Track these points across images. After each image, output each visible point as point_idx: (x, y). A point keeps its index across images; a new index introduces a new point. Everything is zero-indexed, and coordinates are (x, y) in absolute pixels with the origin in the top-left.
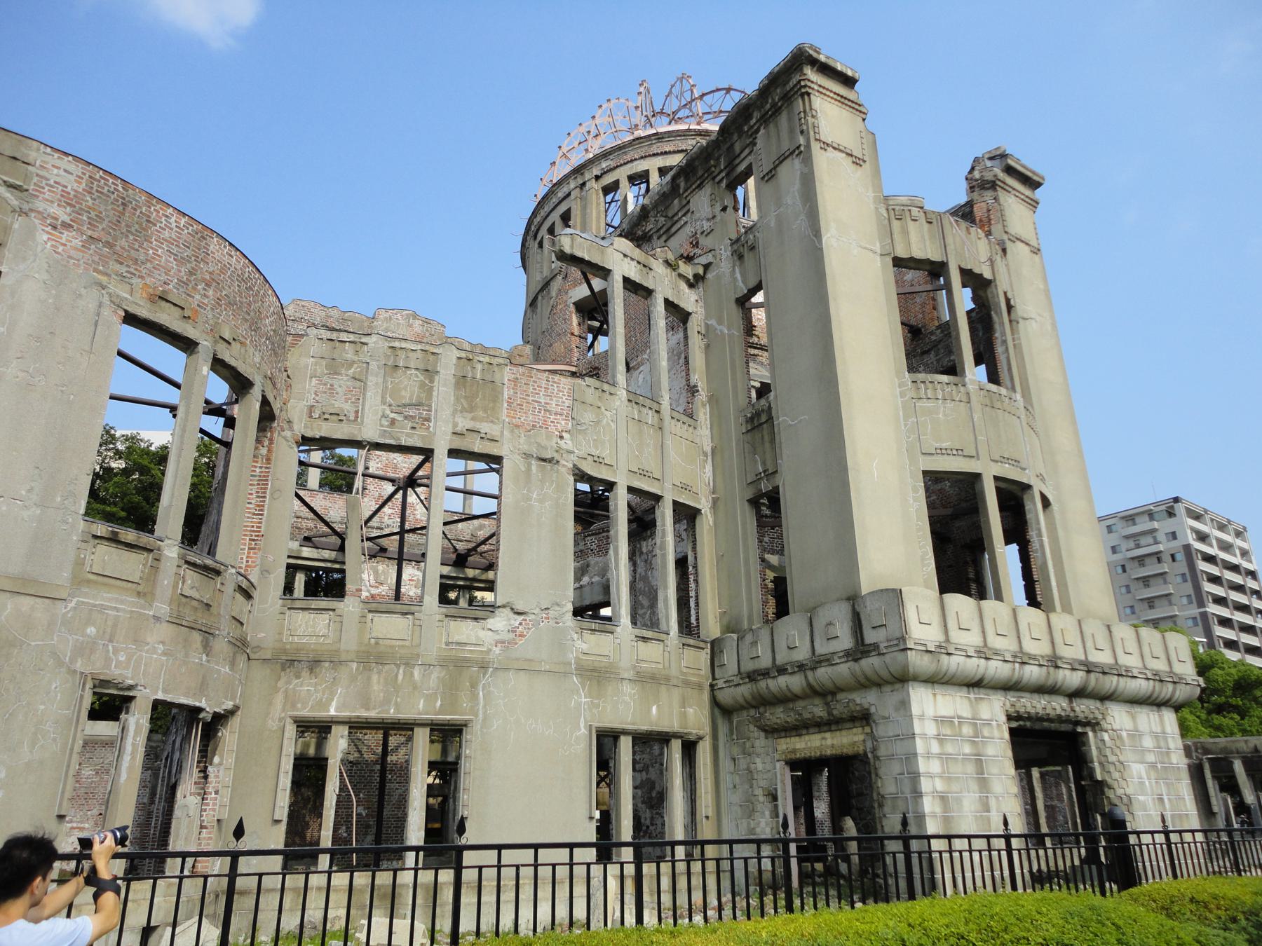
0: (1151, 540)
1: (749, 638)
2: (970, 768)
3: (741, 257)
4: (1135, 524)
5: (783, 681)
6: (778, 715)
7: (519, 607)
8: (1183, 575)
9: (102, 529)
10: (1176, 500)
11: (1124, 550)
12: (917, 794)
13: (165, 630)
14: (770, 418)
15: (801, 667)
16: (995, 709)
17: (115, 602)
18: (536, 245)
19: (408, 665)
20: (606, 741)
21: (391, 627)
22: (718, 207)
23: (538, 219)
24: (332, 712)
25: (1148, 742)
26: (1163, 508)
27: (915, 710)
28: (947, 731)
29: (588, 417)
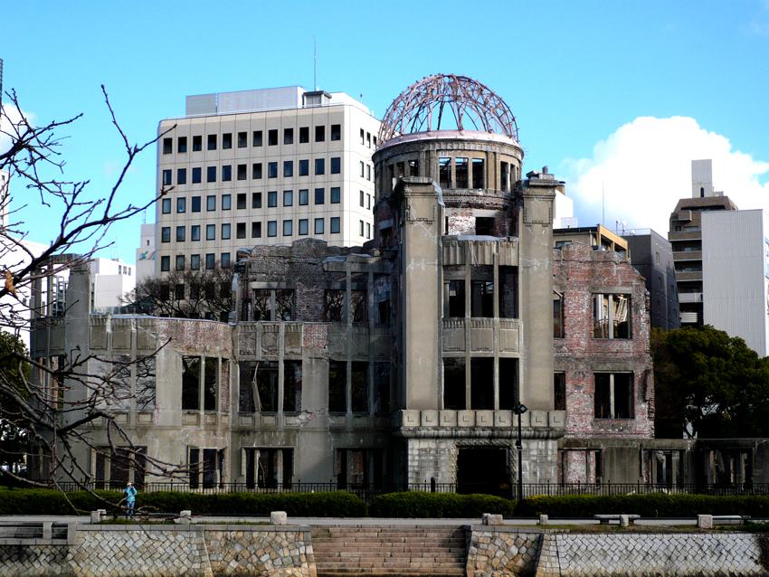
2: (431, 464)
7: (309, 411)
9: (186, 411)
13: (204, 433)
17: (191, 428)
19: (275, 432)
21: (269, 420)
25: (534, 453)
27: (410, 447)
29: (335, 339)
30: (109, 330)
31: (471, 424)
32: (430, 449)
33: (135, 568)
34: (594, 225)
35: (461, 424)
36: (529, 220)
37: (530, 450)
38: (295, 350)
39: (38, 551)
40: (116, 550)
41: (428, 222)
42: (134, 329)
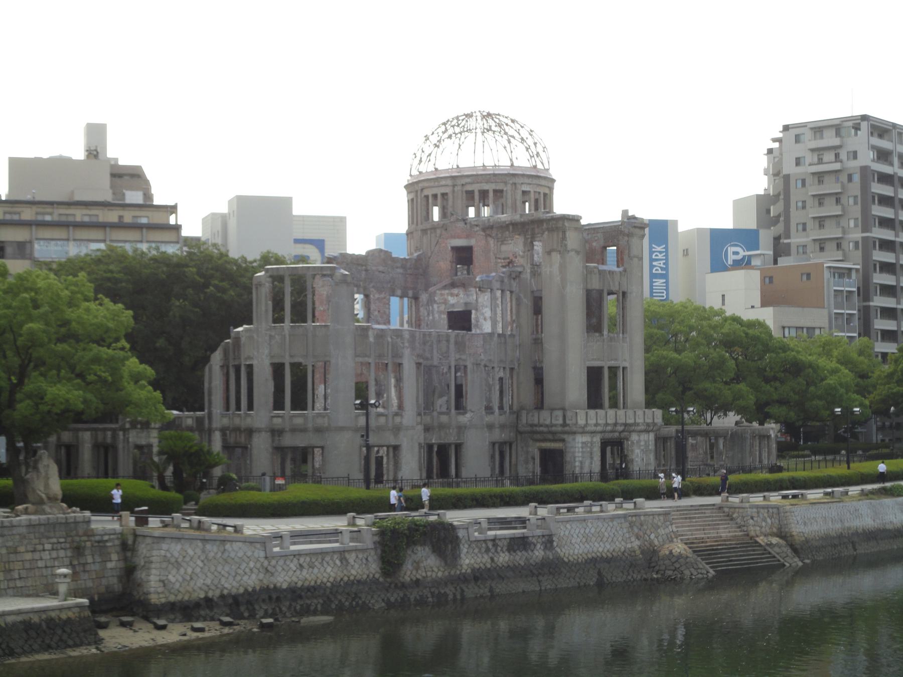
0: (833, 158)
1: (531, 414)
2: (589, 454)
3: (535, 275)
4: (822, 137)
5: (541, 429)
6: (538, 436)
7: (473, 410)
8: (856, 197)
10: (864, 118)
11: (807, 163)
12: (575, 461)
14: (542, 343)
15: (547, 426)
16: (597, 439)
18: (423, 196)
20: (493, 444)
22: (527, 249)
23: (426, 184)
24: (433, 441)
25: (642, 443)
26: (850, 124)
27: (577, 441)
28: (584, 445)
30: (371, 339)
31: (614, 421)
32: (588, 442)
33: (595, 549)
34: (173, 204)
35: (609, 421)
36: (632, 255)
37: (638, 442)
38: (463, 357)
39: (534, 540)
40: (581, 537)
41: (578, 252)
42: (389, 339)
